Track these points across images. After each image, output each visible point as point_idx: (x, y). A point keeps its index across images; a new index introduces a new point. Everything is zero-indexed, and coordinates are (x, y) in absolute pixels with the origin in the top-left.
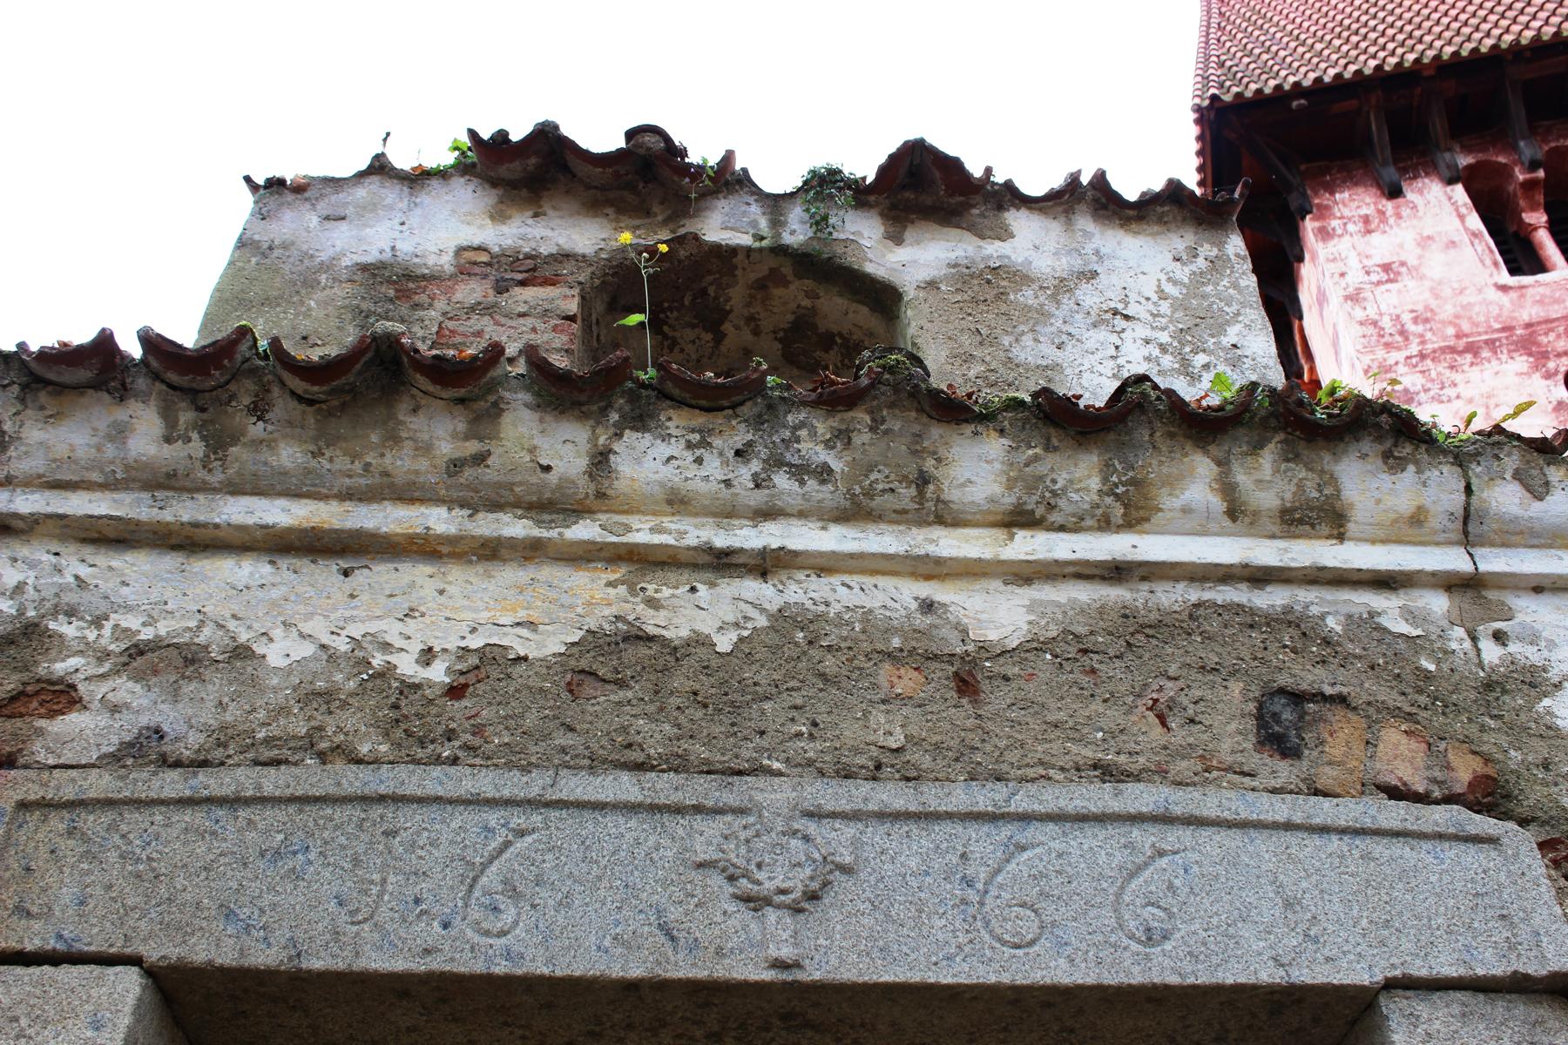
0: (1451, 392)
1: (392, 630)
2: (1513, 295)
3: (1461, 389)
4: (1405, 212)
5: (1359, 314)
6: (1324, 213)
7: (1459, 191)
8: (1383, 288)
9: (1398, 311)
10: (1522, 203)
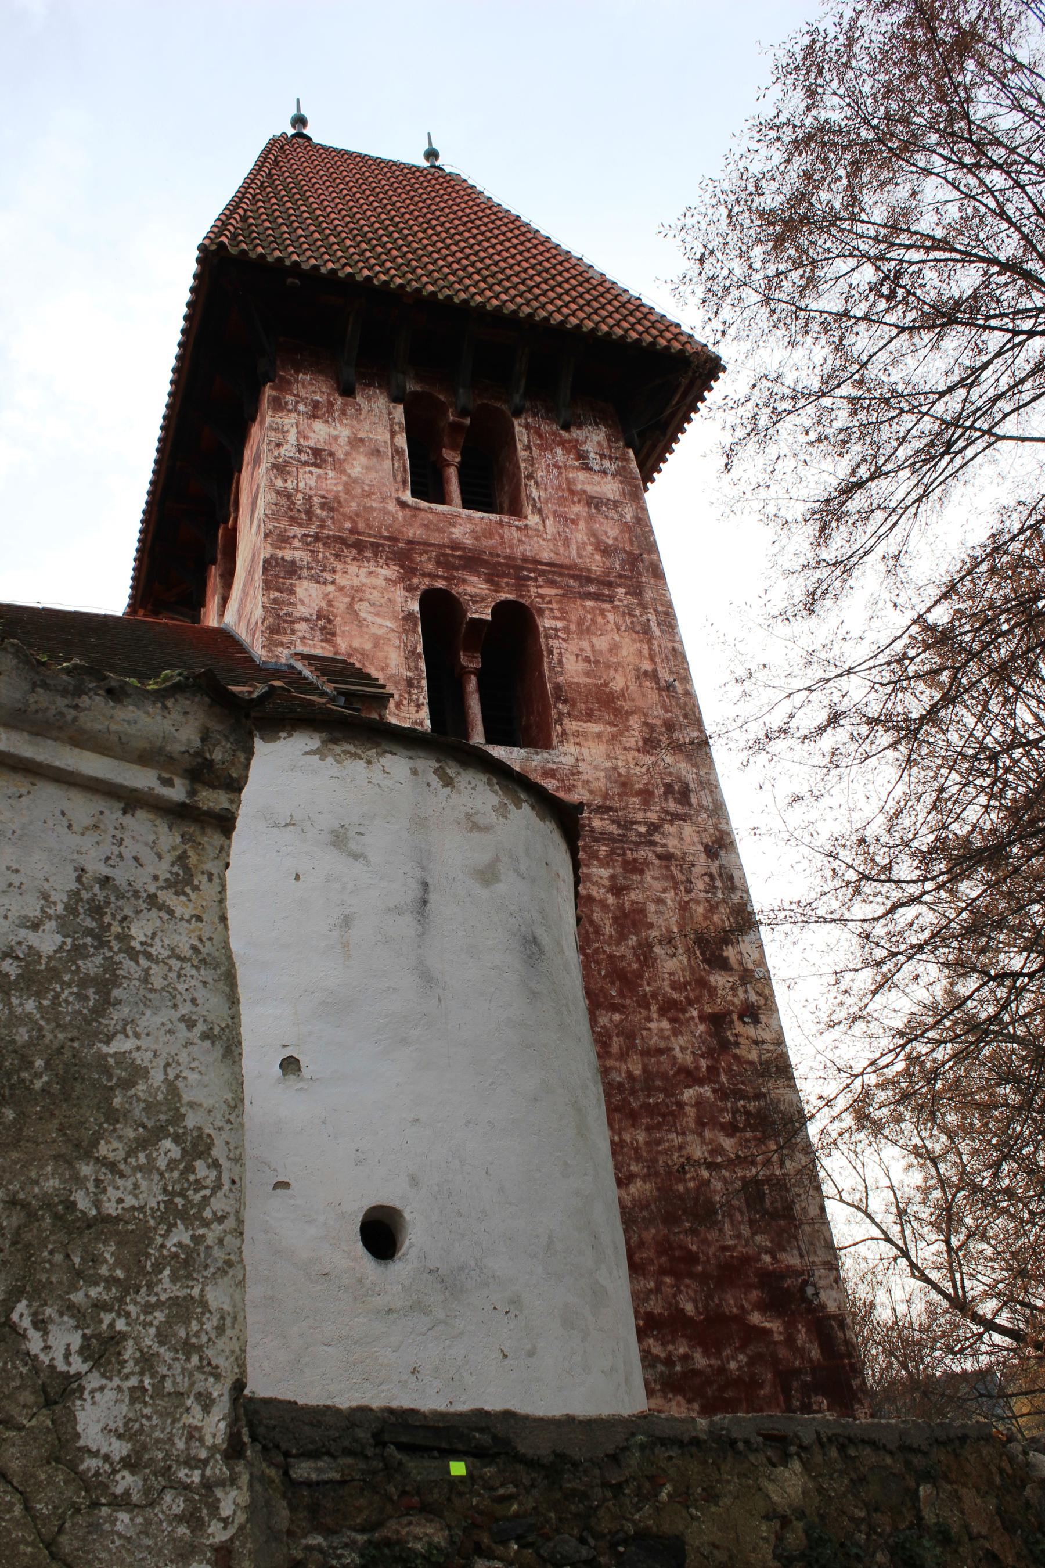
0: (329, 576)
2: (408, 513)
3: (338, 577)
4: (351, 411)
5: (279, 483)
6: (284, 386)
7: (399, 411)
8: (308, 469)
9: (312, 493)
10: (446, 439)
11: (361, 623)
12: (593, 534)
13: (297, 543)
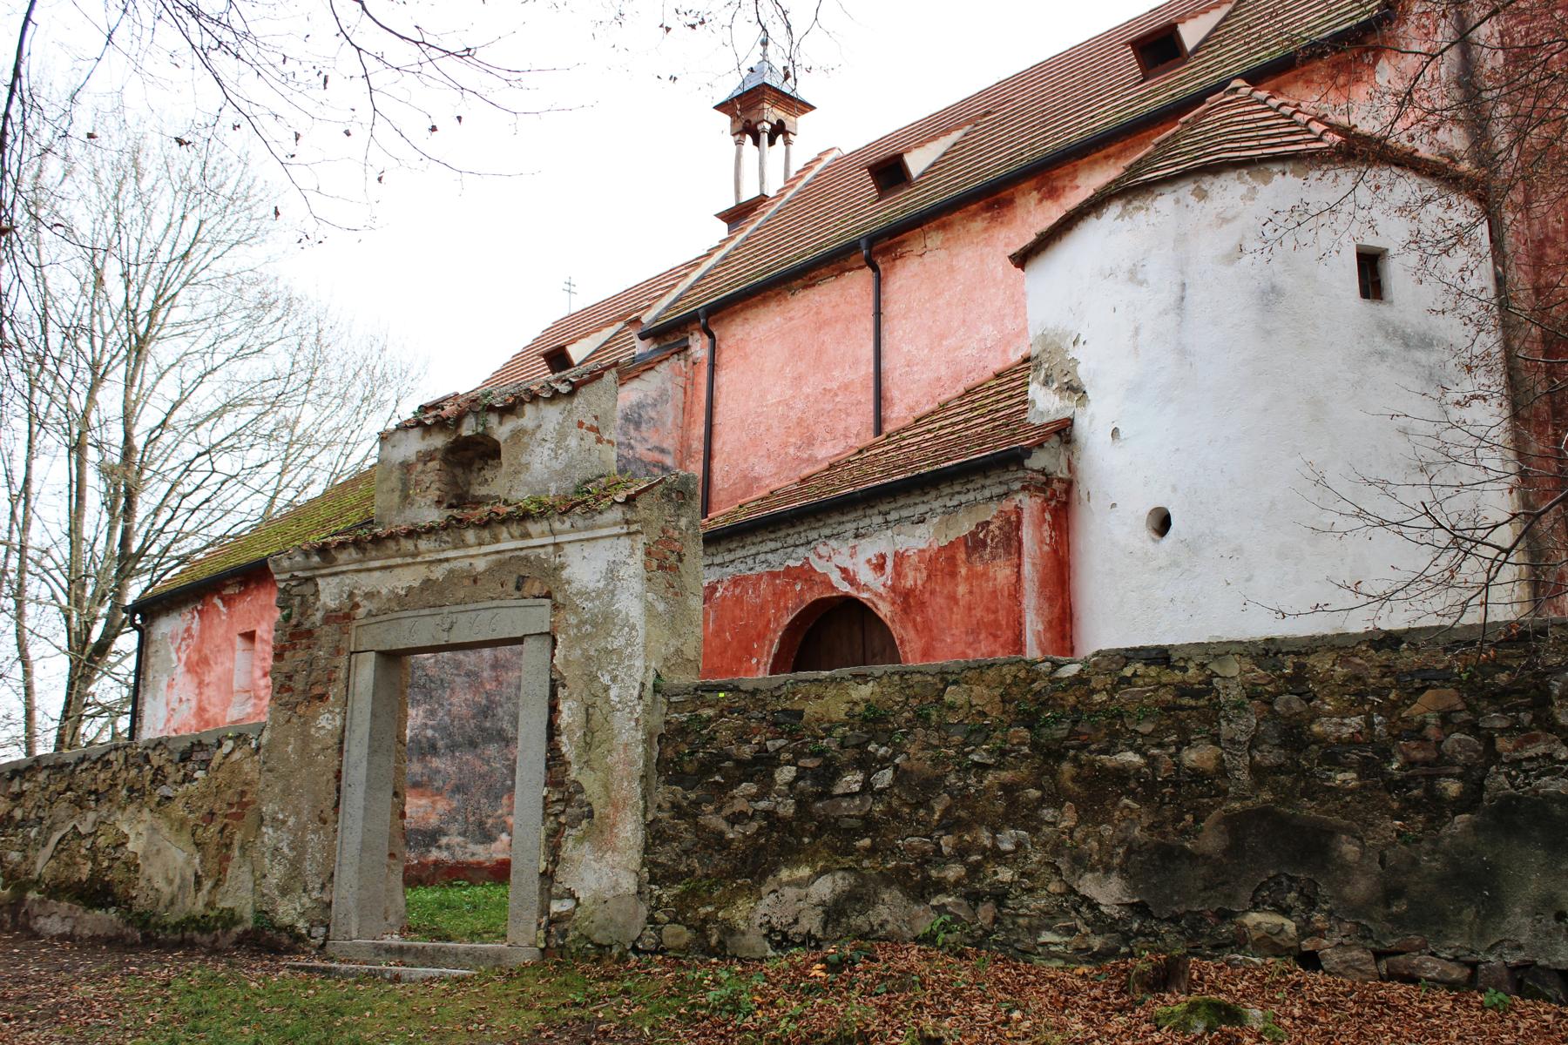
1: (397, 584)
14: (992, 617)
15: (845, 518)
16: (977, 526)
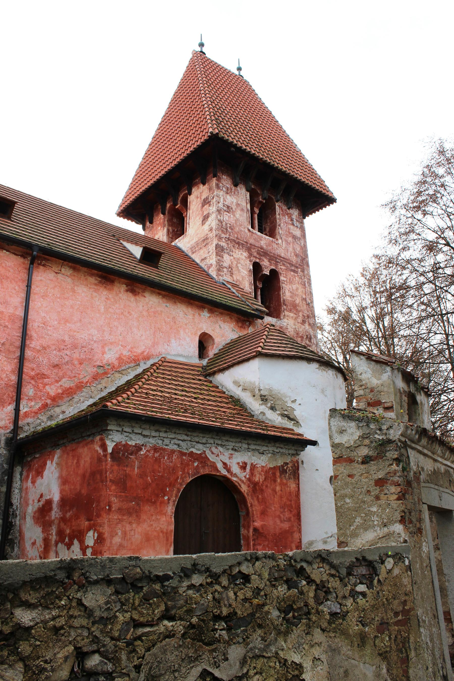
2: (251, 234)
11: (239, 271)
12: (294, 249)
13: (224, 240)
14: (290, 503)
15: (231, 440)
16: (284, 463)
